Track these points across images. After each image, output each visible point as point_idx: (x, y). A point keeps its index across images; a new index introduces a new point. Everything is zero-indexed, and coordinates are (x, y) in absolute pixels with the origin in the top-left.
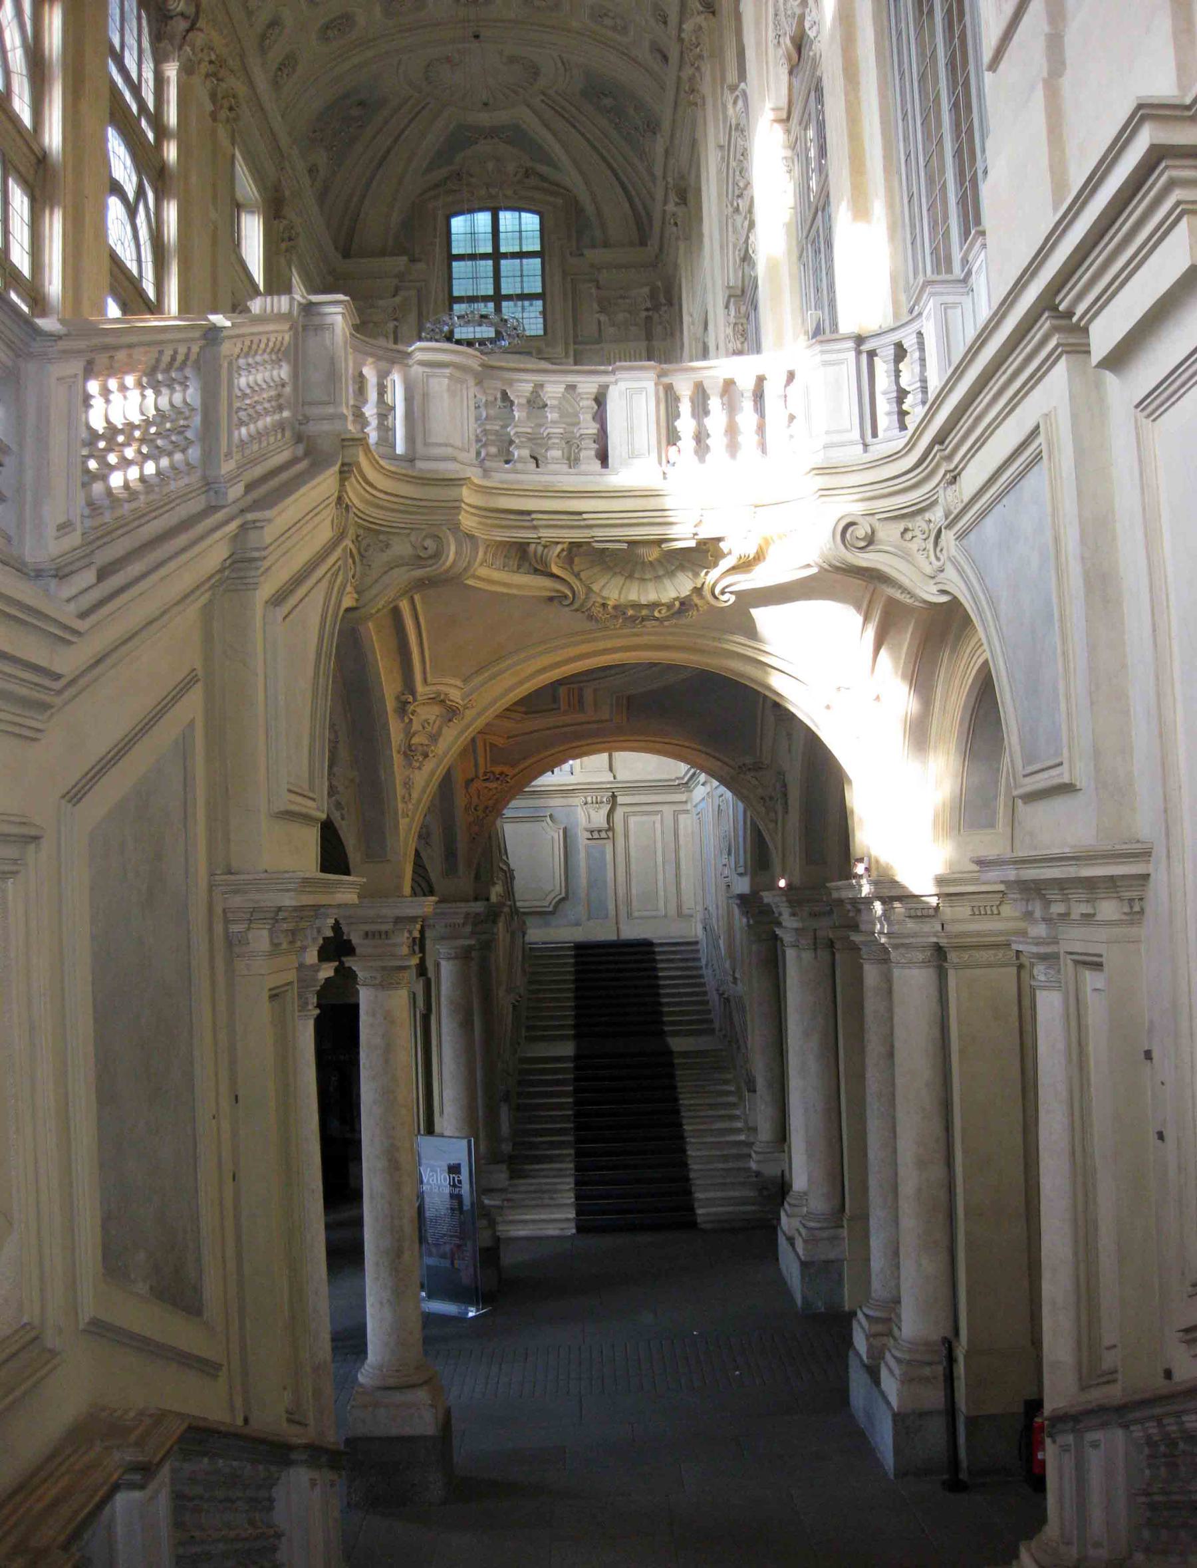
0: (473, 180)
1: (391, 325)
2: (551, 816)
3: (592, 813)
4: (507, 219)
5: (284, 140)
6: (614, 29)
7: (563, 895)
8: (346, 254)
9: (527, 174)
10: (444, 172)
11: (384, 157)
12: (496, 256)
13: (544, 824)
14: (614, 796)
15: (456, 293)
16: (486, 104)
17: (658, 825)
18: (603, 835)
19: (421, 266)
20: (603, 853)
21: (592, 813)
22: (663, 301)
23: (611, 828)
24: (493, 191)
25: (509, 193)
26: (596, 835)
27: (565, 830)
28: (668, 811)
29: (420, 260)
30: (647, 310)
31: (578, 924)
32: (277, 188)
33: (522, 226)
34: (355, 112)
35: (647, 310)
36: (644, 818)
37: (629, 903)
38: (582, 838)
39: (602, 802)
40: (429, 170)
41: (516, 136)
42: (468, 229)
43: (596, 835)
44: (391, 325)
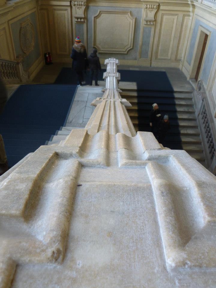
2: (131, 12)
3: (148, 11)
7: (132, 48)
13: (127, 16)
14: (159, 6)
17: (175, 21)
18: (152, 23)
20: (150, 31)
21: (148, 11)
23: (155, 20)
26: (149, 23)
27: (136, 19)
28: (181, 15)
31: (135, 59)
36: (170, 17)
37: (157, 53)
38: (142, 24)
39: (154, 8)
43: (149, 23)
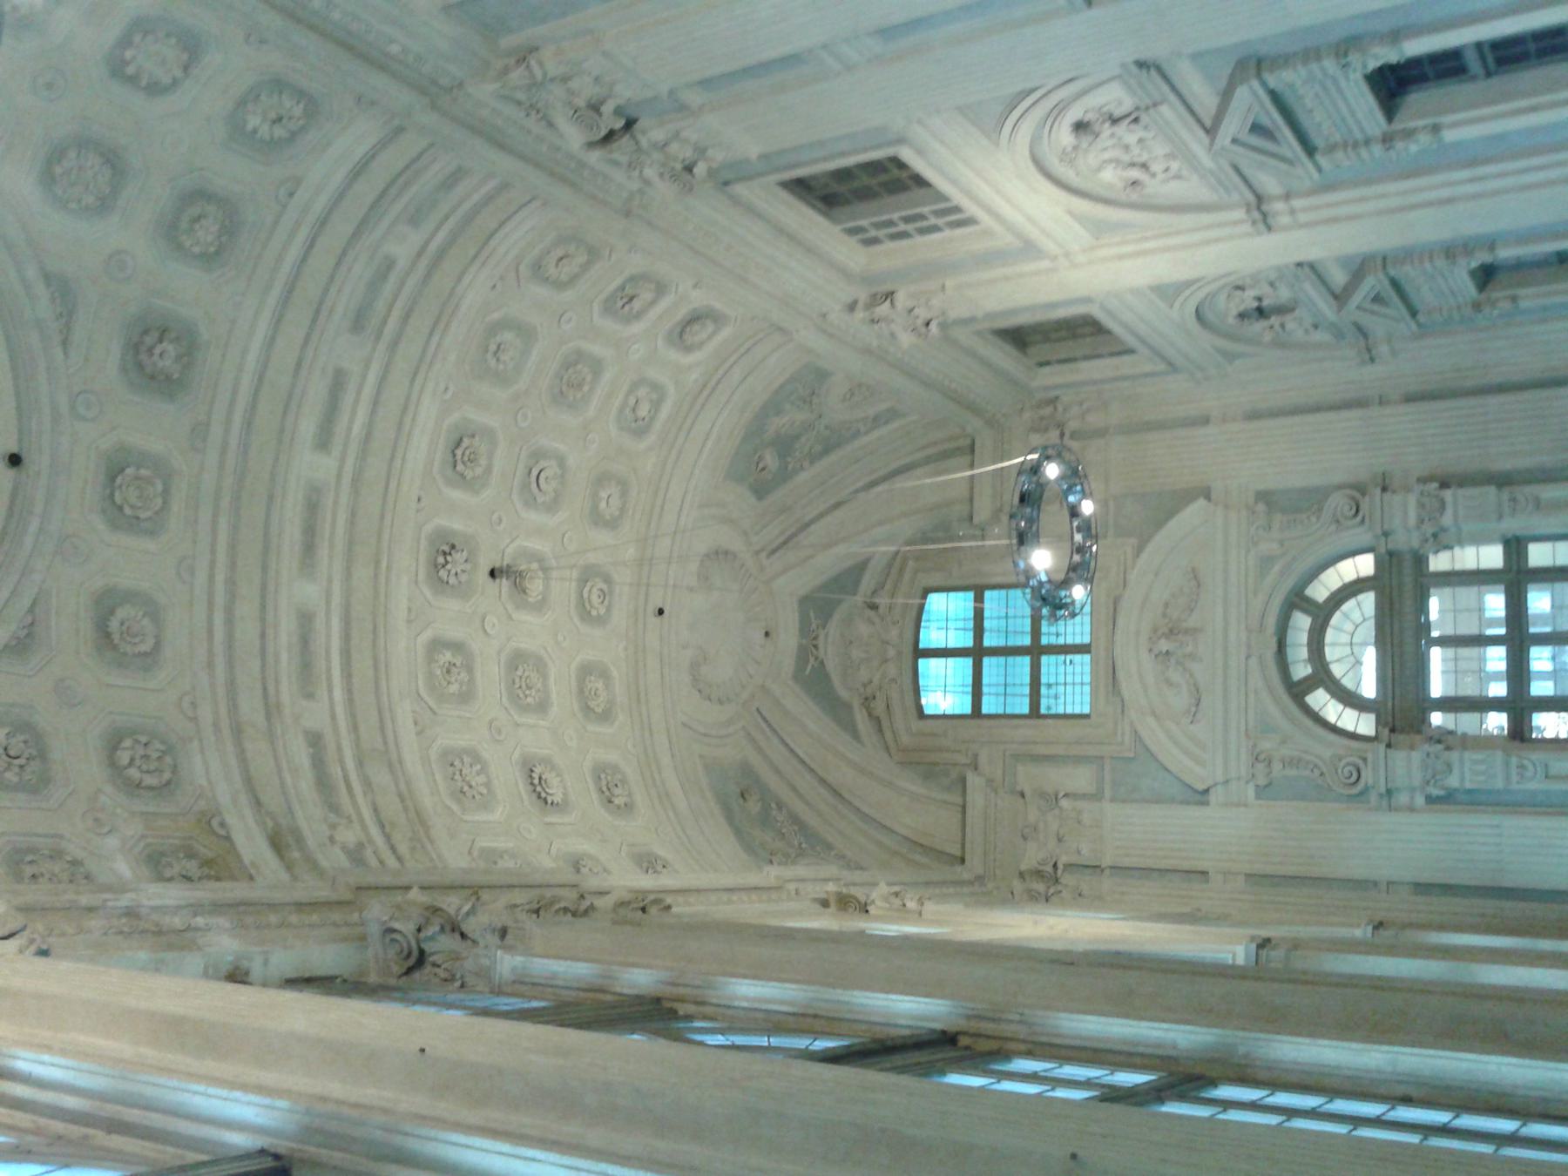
0: (876, 681)
1: (1064, 803)
4: (931, 637)
5: (753, 879)
6: (657, 405)
8: (963, 861)
9: (874, 607)
10: (860, 717)
11: (836, 793)
12: (977, 653)
15: (1026, 710)
16: (767, 634)
19: (983, 760)
22: (1048, 411)
24: (891, 653)
25: (895, 632)
29: (976, 756)
30: (1062, 435)
32: (825, 903)
33: (945, 619)
34: (754, 806)
35: (1062, 435)
40: (855, 735)
41: (818, 607)
42: (943, 690)
44: (1064, 803)
